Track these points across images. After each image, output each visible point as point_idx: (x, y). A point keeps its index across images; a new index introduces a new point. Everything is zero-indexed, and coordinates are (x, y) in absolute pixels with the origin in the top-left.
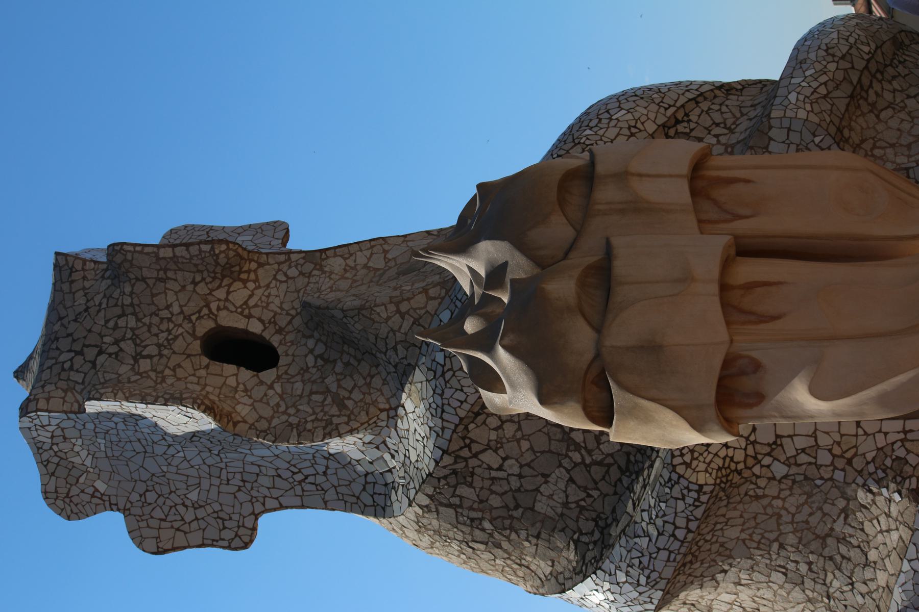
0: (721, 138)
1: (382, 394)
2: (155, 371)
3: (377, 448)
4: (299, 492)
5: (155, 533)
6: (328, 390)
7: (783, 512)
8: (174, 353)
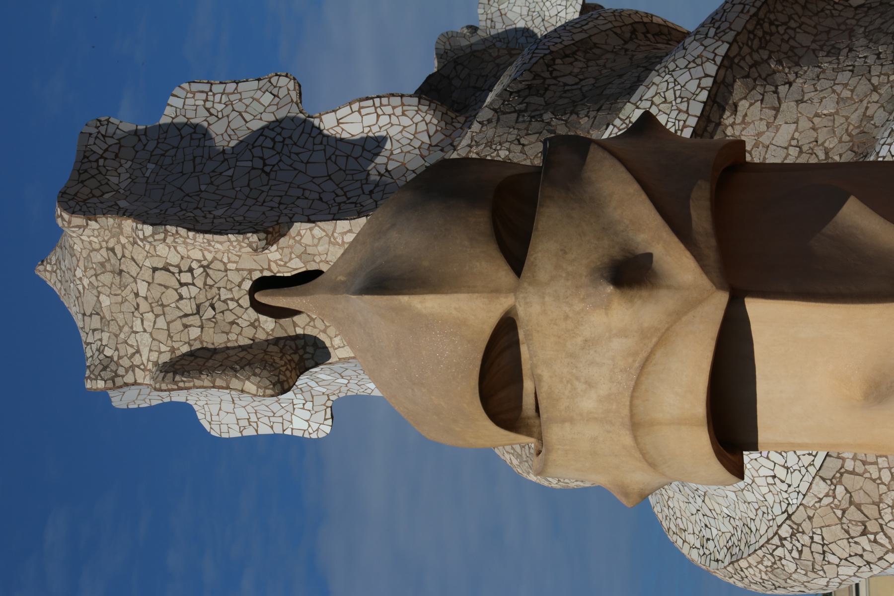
3: (442, 150)
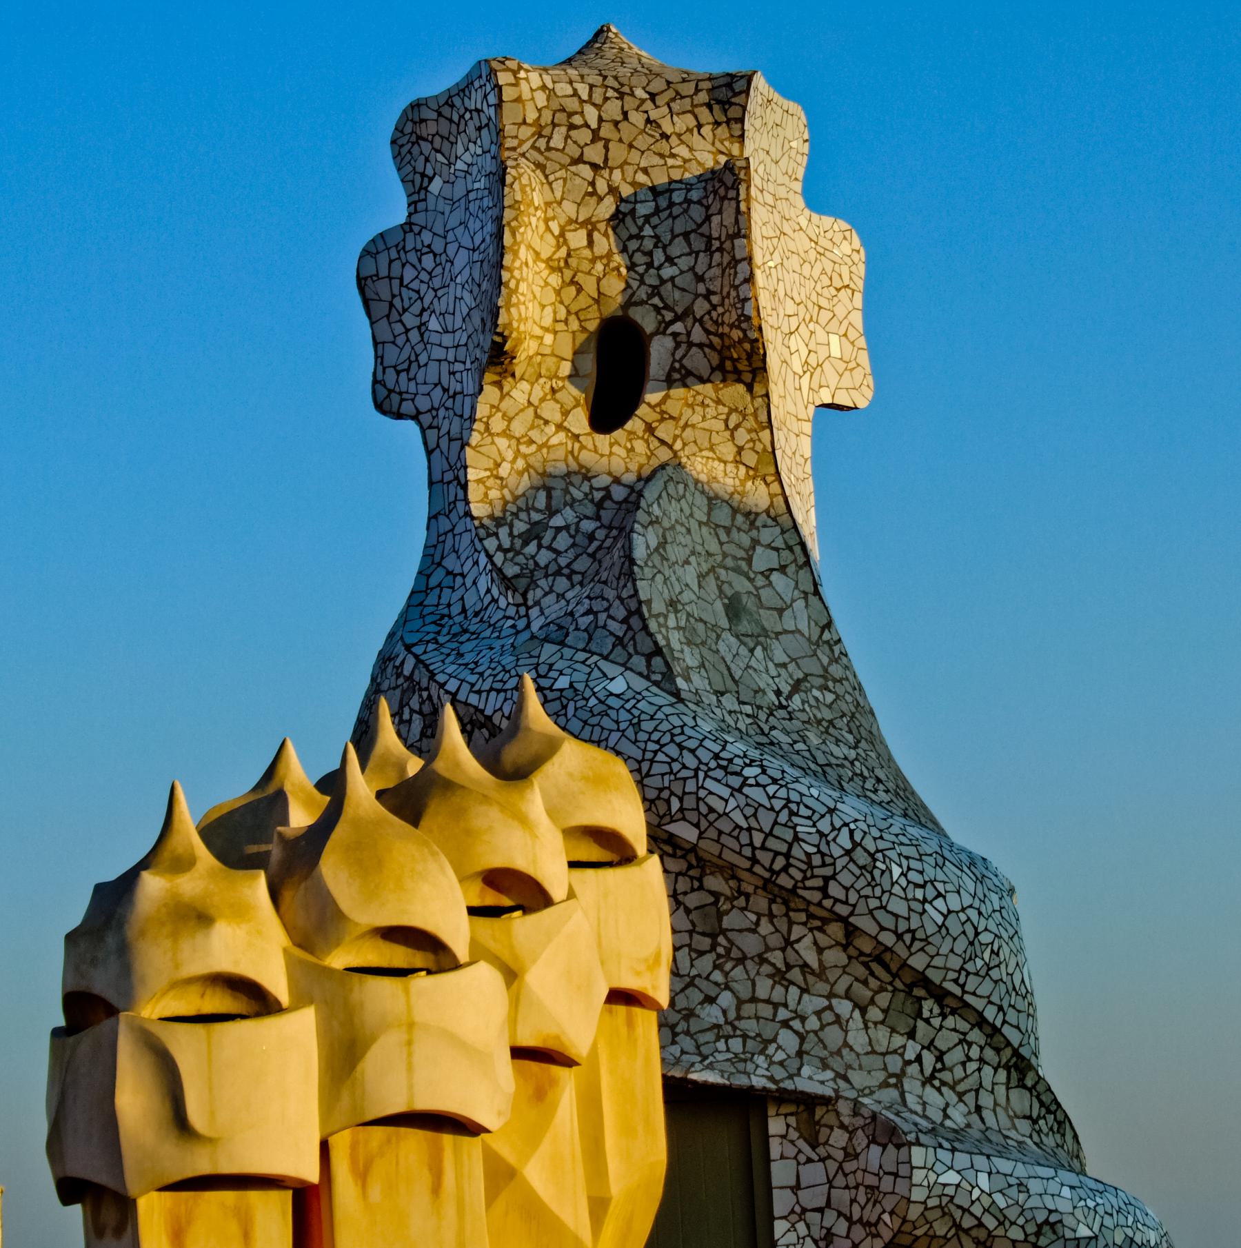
0: (916, 1066)
1: (546, 594)
2: (569, 255)
5: (384, 272)
6: (551, 512)
8: (599, 280)
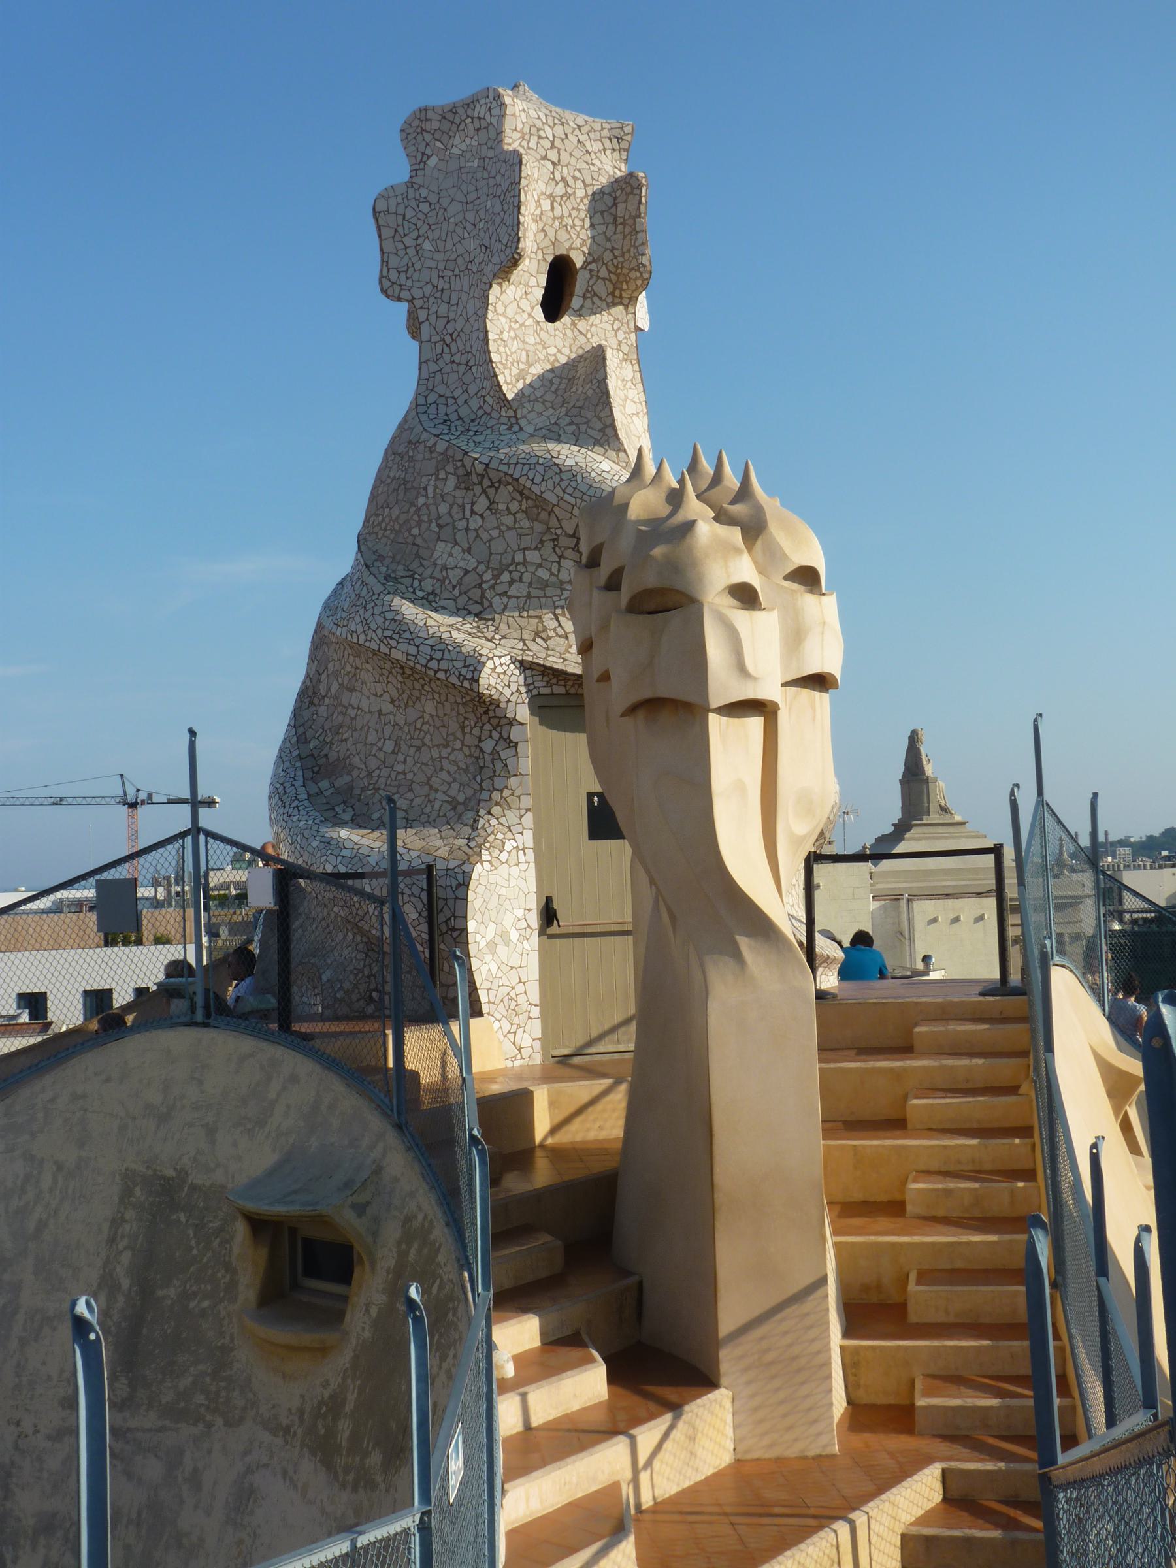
4: (435, 339)
5: (392, 210)
7: (449, 749)
